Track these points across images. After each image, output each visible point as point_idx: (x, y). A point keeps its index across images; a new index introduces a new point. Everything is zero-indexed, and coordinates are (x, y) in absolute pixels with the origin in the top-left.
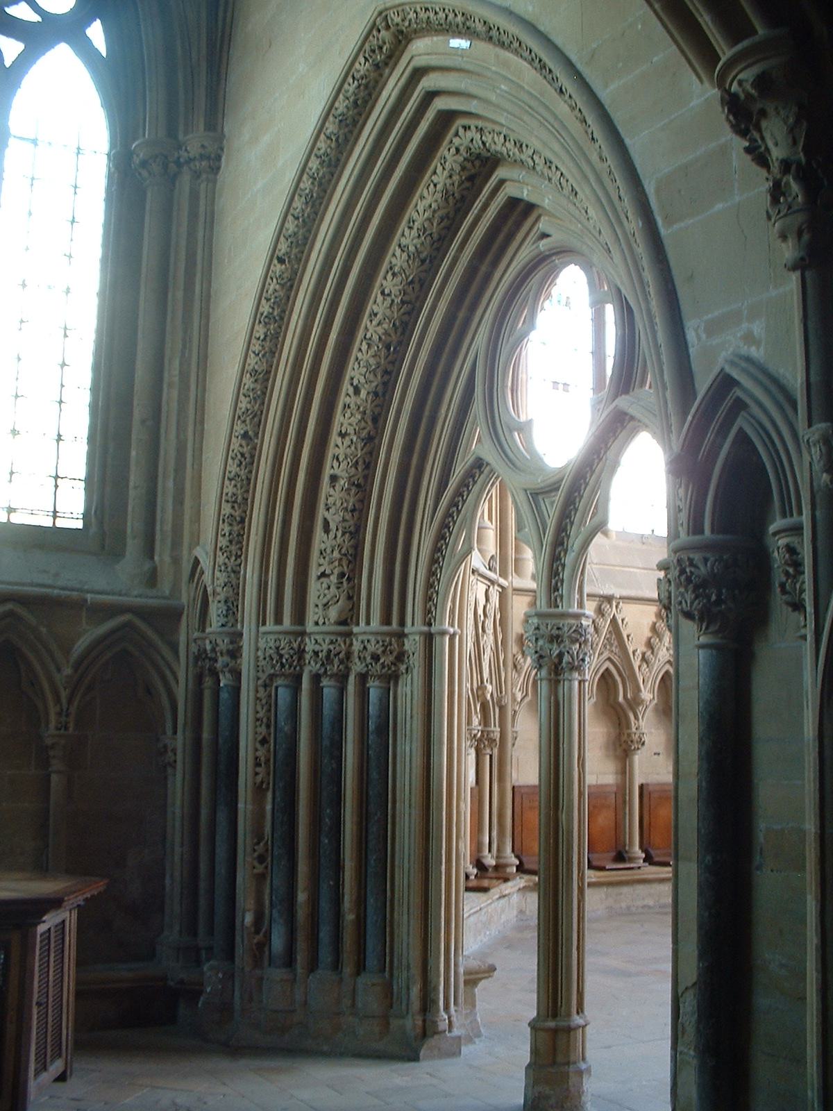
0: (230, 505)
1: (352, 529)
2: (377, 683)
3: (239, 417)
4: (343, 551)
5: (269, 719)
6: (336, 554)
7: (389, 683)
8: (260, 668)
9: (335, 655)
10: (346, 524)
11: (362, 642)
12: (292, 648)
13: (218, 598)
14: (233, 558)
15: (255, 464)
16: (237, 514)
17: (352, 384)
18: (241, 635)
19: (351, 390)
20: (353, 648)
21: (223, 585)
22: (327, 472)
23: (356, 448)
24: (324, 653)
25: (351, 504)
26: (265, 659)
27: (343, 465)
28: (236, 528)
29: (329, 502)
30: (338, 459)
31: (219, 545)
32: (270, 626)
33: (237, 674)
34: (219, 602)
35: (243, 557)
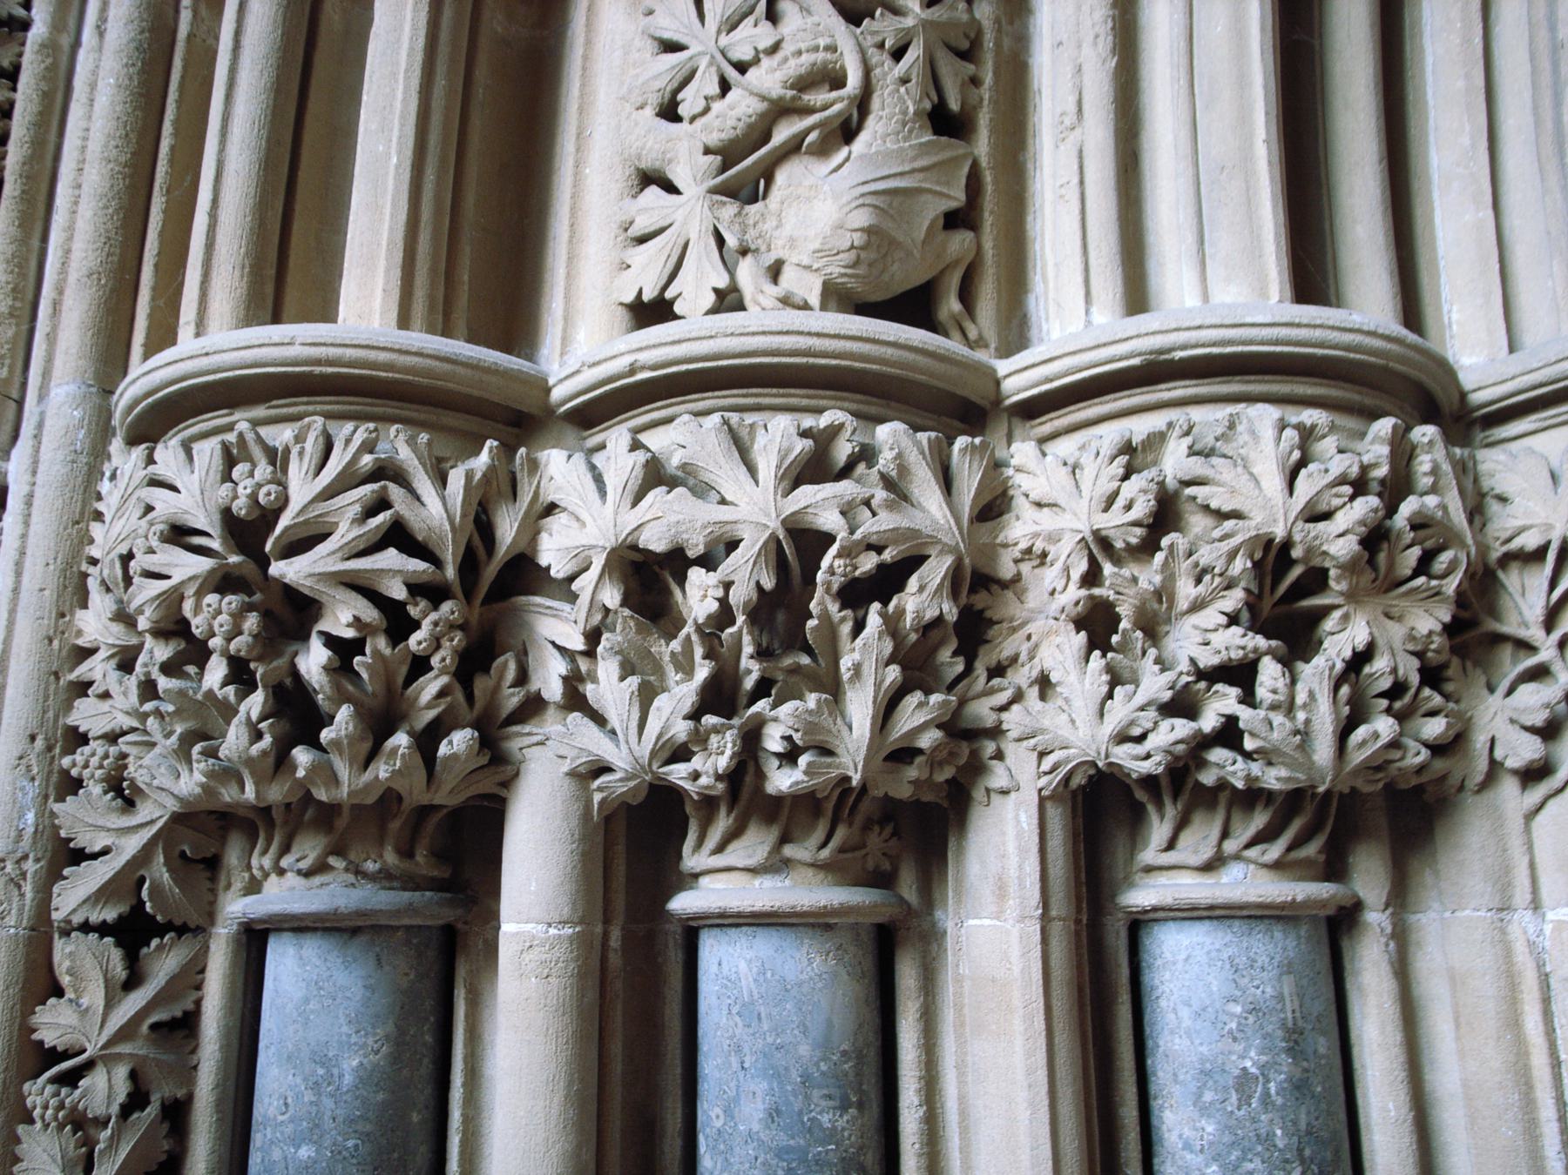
8: (89, 761)
9: (856, 595)
11: (1133, 457)
12: (399, 536)
20: (1021, 528)
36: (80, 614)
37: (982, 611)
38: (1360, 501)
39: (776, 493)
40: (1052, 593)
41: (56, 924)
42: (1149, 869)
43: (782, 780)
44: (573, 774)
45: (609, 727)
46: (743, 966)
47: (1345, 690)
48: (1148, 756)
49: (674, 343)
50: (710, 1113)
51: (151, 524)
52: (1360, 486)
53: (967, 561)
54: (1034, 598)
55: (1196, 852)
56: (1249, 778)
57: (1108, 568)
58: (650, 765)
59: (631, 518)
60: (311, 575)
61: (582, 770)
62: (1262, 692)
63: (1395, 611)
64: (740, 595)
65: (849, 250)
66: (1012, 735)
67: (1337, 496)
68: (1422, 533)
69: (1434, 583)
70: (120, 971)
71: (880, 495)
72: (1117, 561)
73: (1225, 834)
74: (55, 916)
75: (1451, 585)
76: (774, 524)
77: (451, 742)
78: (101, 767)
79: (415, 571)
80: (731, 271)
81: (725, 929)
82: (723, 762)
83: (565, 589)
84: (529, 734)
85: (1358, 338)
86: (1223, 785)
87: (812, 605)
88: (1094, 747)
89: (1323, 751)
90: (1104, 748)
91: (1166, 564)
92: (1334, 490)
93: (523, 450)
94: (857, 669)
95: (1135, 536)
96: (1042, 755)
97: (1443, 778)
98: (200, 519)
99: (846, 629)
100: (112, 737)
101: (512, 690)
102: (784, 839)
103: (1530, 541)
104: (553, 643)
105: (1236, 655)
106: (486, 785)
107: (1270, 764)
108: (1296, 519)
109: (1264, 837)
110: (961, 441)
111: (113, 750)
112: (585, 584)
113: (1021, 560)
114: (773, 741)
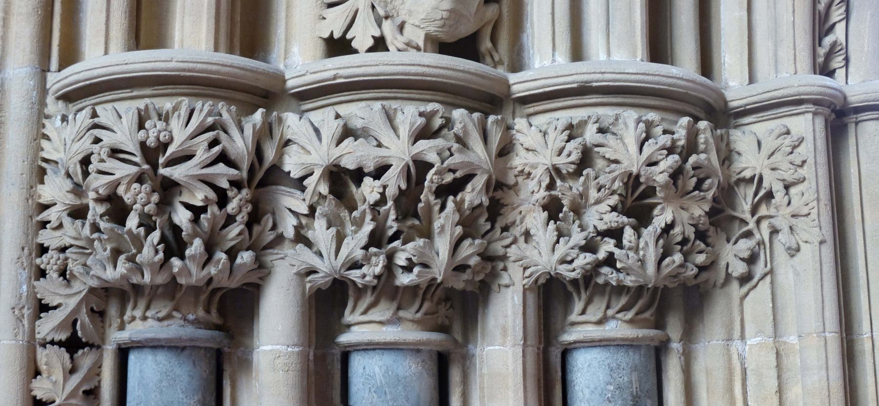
2: (617, 329)
7: (659, 324)
9: (444, 192)
11: (573, 131)
12: (224, 158)
20: (519, 160)
24: (393, 181)
26: (78, 213)
36: (40, 187)
37: (499, 200)
38: (671, 156)
39: (408, 144)
40: (533, 193)
41: (38, 340)
42: (573, 324)
43: (404, 279)
44: (298, 274)
45: (315, 249)
46: (377, 369)
47: (661, 242)
48: (574, 270)
49: (358, 67)
51: (101, 148)
52: (671, 150)
53: (494, 177)
54: (523, 195)
55: (594, 315)
56: (618, 280)
57: (559, 183)
58: (340, 270)
59: (336, 152)
60: (187, 176)
61: (302, 272)
62: (625, 242)
63: (685, 206)
64: (391, 192)
65: (440, 20)
66: (512, 259)
67: (661, 155)
68: (698, 171)
69: (702, 194)
70: (69, 365)
71: (456, 146)
72: (563, 178)
73: (608, 307)
74: (38, 336)
75: (710, 195)
76: (408, 159)
77: (242, 257)
78: (56, 264)
79: (233, 175)
80: (380, 26)
81: (367, 351)
82: (378, 270)
83: (300, 184)
84: (277, 254)
85: (674, 81)
86: (607, 284)
87: (422, 197)
88: (549, 266)
89: (651, 268)
90: (554, 266)
91: (584, 183)
92: (660, 152)
93: (275, 113)
94: (442, 228)
95: (572, 168)
96: (525, 269)
97: (706, 281)
98: (131, 146)
99: (437, 208)
100: (63, 250)
101: (270, 232)
102: (399, 308)
103: (747, 174)
104: (290, 210)
105: (614, 225)
106: (253, 279)
107: (628, 274)
108: (642, 164)
109: (624, 309)
110: (491, 118)
111: (62, 256)
112: (310, 182)
113: (518, 176)
114: (401, 260)
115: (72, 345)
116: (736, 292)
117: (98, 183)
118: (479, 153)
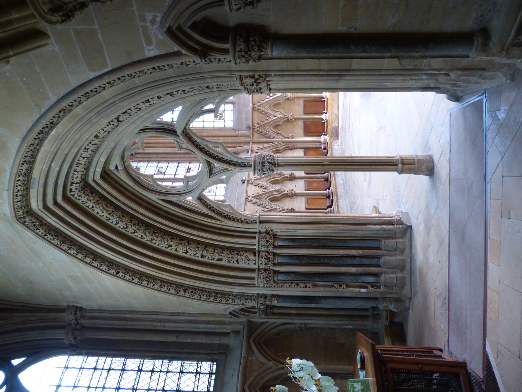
0: (210, 298)
1: (221, 250)
2: (277, 242)
3: (178, 293)
4: (229, 253)
5: (289, 283)
6: (230, 256)
7: (276, 238)
8: (271, 286)
10: (219, 252)
11: (262, 246)
12: (264, 273)
13: (245, 303)
14: (230, 296)
15: (196, 288)
16: (214, 295)
17: (168, 247)
18: (258, 294)
19: (170, 248)
20: (264, 250)
21: (240, 301)
22: (200, 259)
23: (192, 247)
24: (266, 260)
25: (212, 250)
26: (267, 284)
27: (198, 252)
28: (219, 296)
29: (211, 258)
30: (195, 254)
31: (225, 302)
32: (255, 282)
33: (273, 296)
34: (246, 302)
35: (230, 293)
50: (284, 262)
98: (263, 280)
115: (277, 284)
116: (274, 232)
117: (266, 282)
118: (264, 254)
